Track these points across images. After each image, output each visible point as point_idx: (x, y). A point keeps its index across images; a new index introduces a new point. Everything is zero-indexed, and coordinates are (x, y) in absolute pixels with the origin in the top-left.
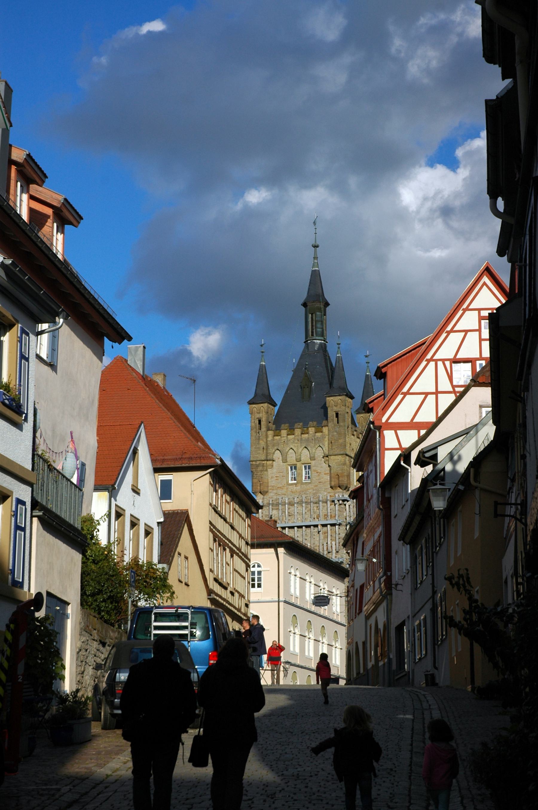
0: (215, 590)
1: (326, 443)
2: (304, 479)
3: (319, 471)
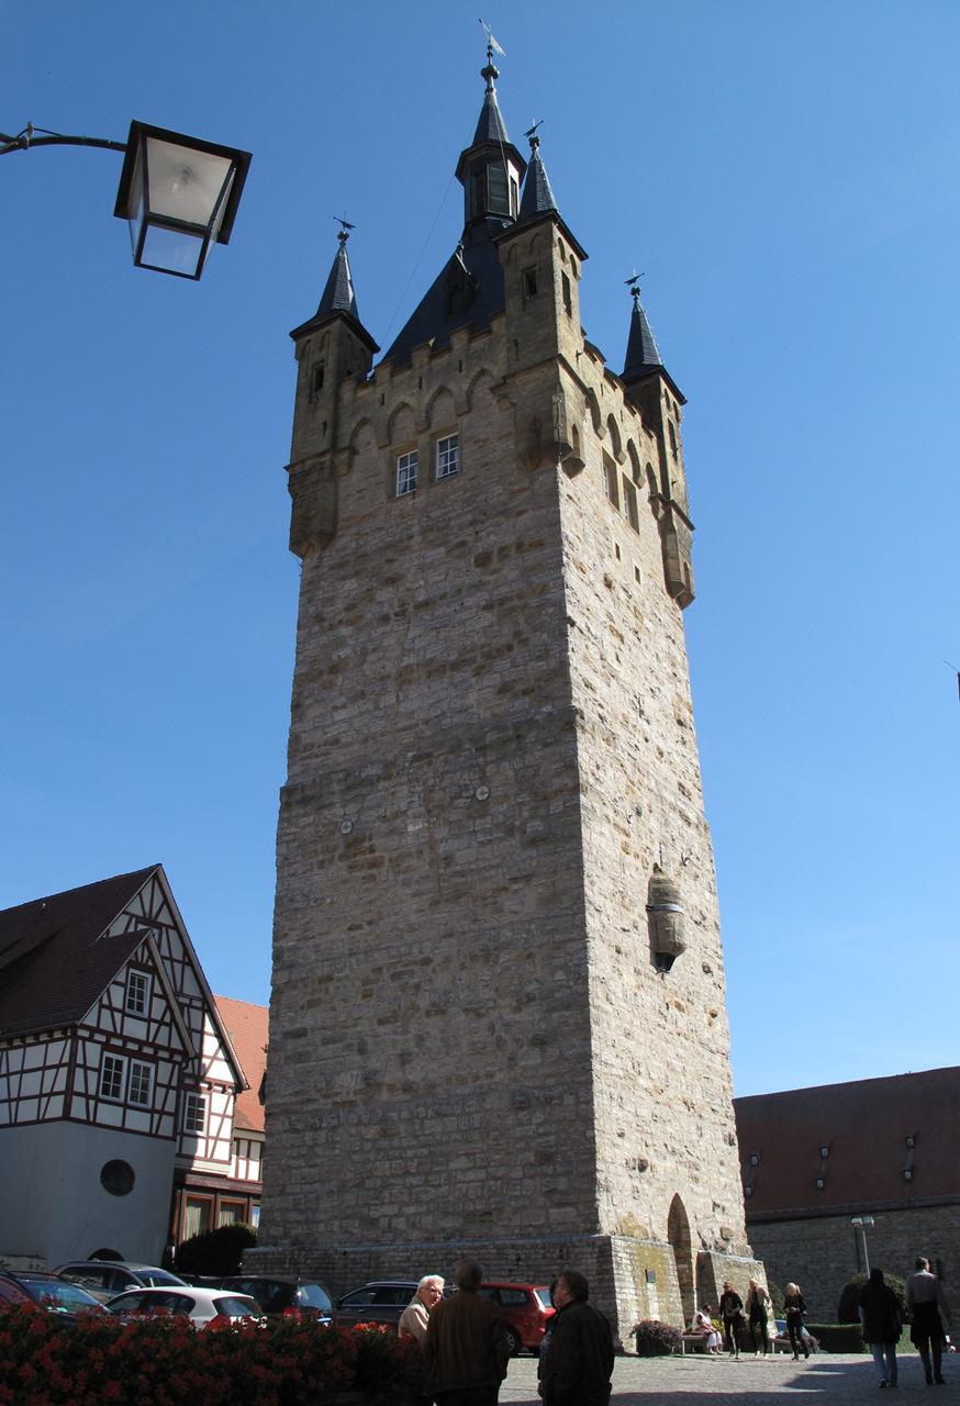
2: (438, 476)
3: (481, 437)
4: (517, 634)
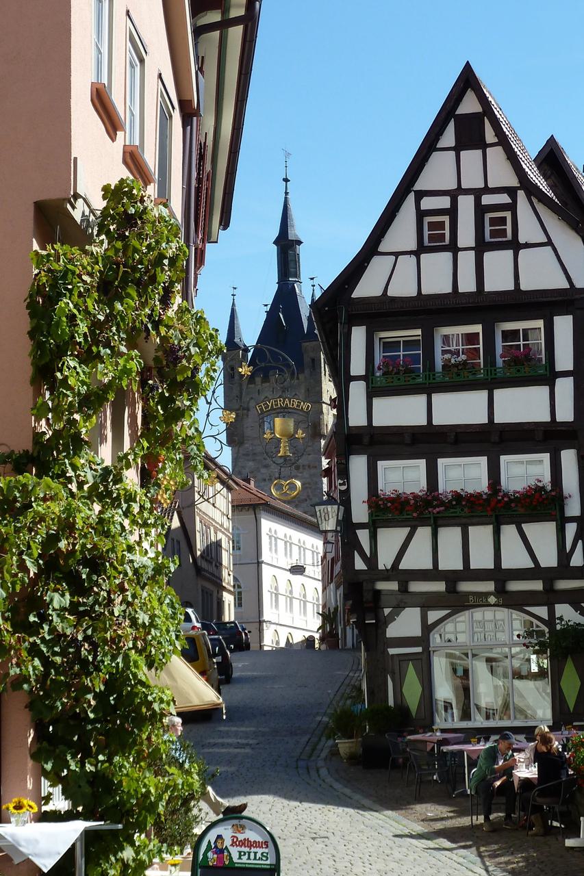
0: (203, 566)
1: (303, 391)
4: (308, 496)
